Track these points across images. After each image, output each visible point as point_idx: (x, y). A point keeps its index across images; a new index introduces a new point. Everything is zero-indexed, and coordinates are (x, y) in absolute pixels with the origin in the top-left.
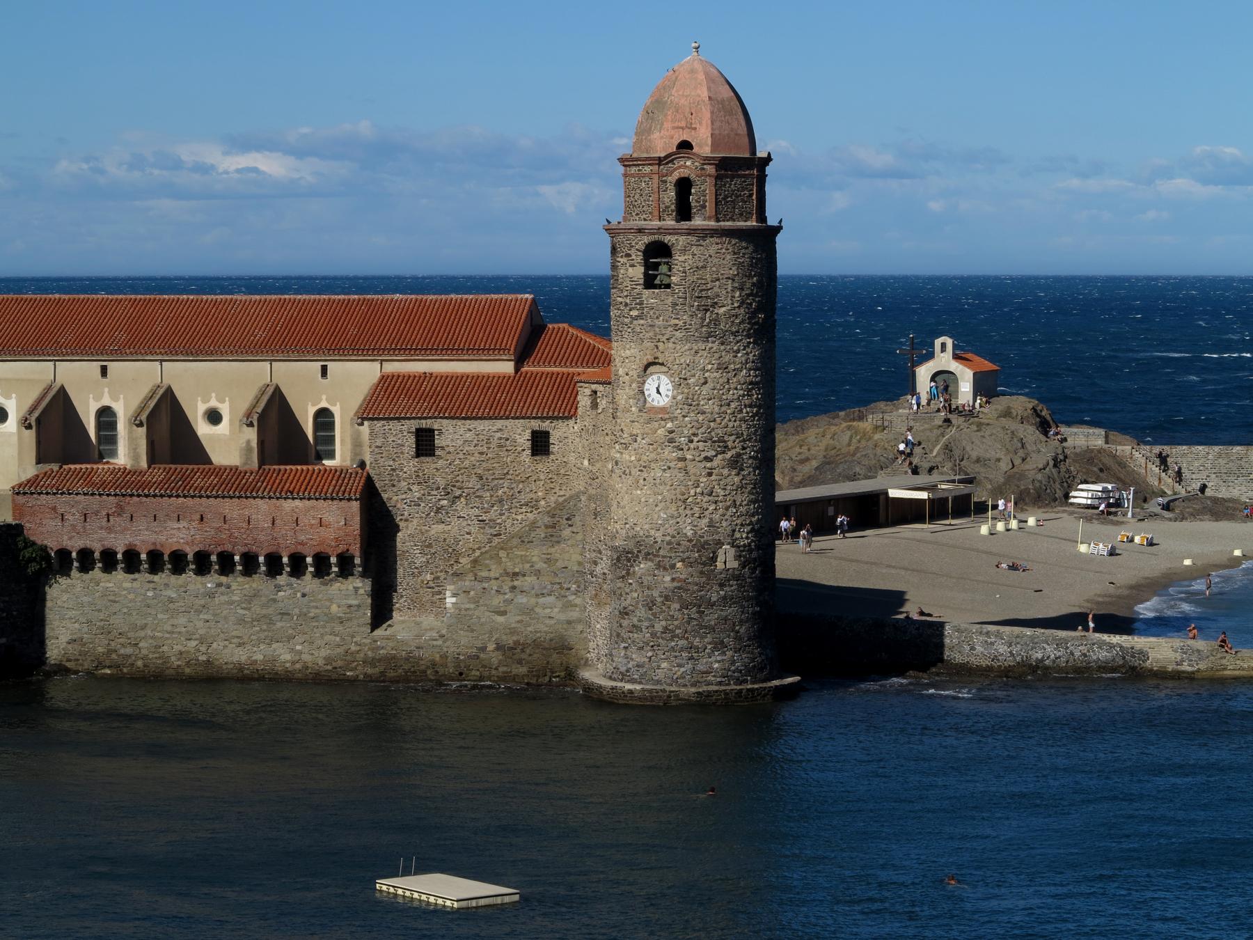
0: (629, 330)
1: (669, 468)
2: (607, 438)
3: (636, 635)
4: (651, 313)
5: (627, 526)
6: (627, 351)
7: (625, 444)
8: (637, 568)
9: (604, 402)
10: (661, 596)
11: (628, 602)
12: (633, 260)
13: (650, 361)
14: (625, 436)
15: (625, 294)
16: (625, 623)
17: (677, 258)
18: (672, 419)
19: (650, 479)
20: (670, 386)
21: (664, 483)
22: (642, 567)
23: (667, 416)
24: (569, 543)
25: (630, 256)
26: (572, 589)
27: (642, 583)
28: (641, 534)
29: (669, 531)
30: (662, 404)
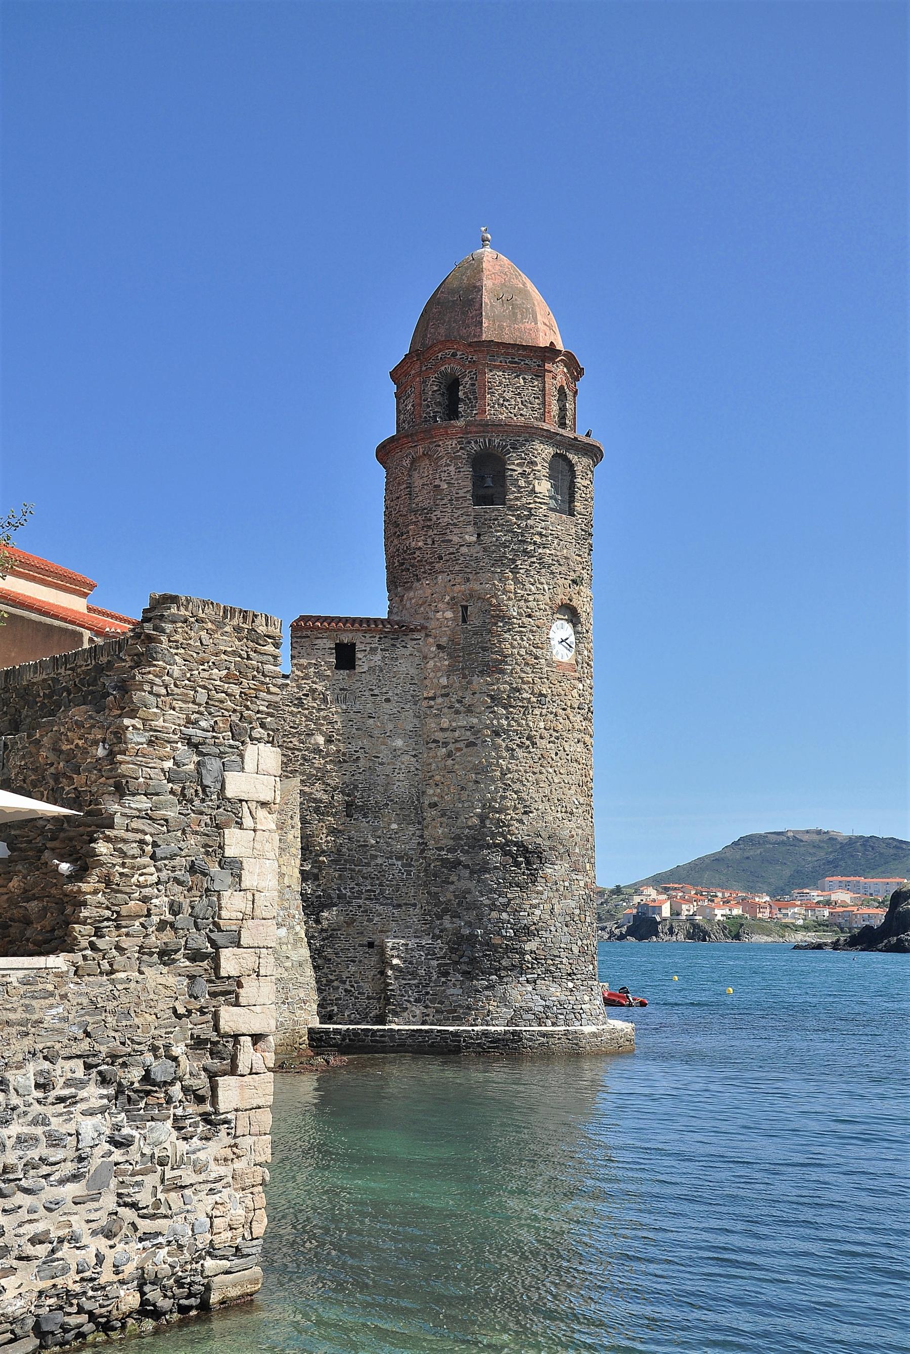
0: (534, 559)
2: (385, 705)
4: (556, 541)
5: (530, 814)
6: (528, 586)
7: (523, 707)
8: (549, 871)
11: (536, 919)
13: (565, 602)
14: (525, 695)
15: (526, 513)
16: (527, 947)
17: (579, 480)
19: (561, 753)
20: (572, 639)
22: (556, 870)
23: (577, 675)
24: (293, 850)
26: (297, 916)
27: (557, 890)
30: (565, 660)
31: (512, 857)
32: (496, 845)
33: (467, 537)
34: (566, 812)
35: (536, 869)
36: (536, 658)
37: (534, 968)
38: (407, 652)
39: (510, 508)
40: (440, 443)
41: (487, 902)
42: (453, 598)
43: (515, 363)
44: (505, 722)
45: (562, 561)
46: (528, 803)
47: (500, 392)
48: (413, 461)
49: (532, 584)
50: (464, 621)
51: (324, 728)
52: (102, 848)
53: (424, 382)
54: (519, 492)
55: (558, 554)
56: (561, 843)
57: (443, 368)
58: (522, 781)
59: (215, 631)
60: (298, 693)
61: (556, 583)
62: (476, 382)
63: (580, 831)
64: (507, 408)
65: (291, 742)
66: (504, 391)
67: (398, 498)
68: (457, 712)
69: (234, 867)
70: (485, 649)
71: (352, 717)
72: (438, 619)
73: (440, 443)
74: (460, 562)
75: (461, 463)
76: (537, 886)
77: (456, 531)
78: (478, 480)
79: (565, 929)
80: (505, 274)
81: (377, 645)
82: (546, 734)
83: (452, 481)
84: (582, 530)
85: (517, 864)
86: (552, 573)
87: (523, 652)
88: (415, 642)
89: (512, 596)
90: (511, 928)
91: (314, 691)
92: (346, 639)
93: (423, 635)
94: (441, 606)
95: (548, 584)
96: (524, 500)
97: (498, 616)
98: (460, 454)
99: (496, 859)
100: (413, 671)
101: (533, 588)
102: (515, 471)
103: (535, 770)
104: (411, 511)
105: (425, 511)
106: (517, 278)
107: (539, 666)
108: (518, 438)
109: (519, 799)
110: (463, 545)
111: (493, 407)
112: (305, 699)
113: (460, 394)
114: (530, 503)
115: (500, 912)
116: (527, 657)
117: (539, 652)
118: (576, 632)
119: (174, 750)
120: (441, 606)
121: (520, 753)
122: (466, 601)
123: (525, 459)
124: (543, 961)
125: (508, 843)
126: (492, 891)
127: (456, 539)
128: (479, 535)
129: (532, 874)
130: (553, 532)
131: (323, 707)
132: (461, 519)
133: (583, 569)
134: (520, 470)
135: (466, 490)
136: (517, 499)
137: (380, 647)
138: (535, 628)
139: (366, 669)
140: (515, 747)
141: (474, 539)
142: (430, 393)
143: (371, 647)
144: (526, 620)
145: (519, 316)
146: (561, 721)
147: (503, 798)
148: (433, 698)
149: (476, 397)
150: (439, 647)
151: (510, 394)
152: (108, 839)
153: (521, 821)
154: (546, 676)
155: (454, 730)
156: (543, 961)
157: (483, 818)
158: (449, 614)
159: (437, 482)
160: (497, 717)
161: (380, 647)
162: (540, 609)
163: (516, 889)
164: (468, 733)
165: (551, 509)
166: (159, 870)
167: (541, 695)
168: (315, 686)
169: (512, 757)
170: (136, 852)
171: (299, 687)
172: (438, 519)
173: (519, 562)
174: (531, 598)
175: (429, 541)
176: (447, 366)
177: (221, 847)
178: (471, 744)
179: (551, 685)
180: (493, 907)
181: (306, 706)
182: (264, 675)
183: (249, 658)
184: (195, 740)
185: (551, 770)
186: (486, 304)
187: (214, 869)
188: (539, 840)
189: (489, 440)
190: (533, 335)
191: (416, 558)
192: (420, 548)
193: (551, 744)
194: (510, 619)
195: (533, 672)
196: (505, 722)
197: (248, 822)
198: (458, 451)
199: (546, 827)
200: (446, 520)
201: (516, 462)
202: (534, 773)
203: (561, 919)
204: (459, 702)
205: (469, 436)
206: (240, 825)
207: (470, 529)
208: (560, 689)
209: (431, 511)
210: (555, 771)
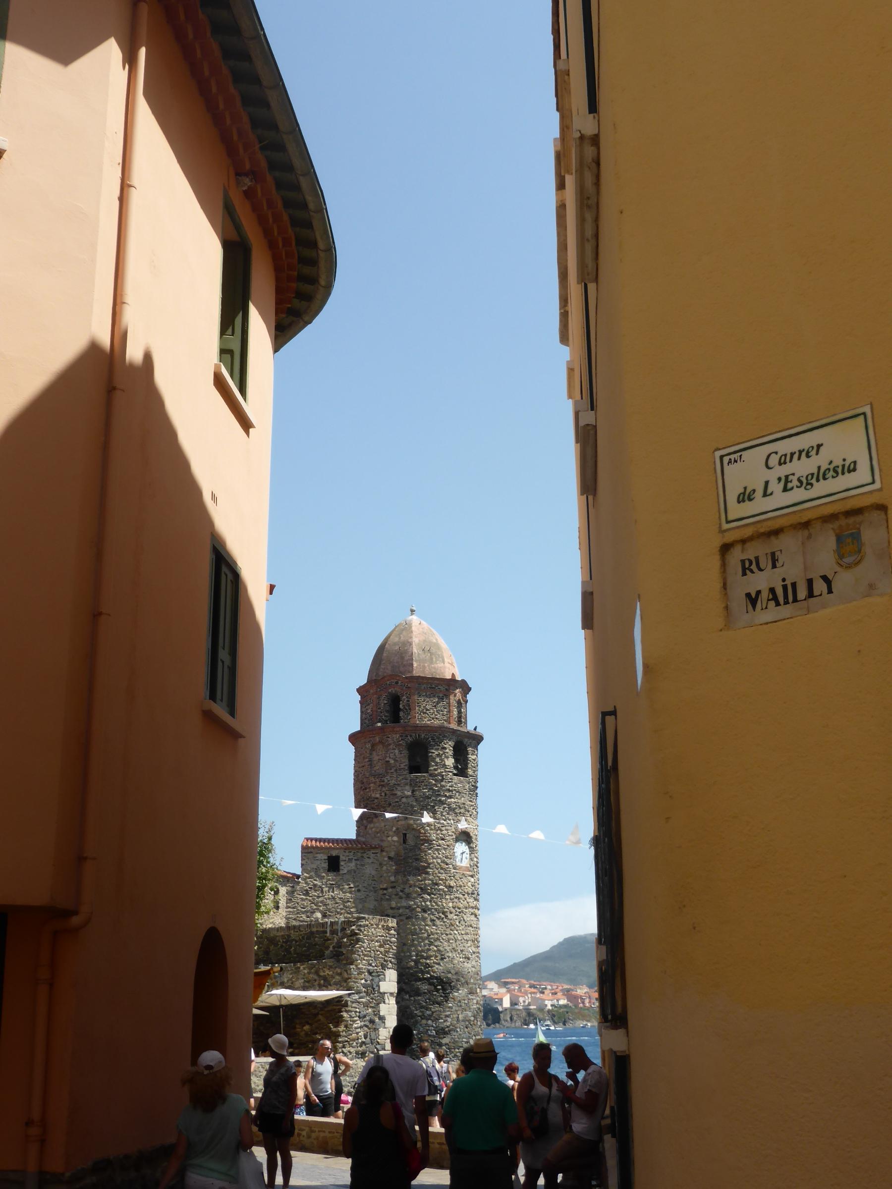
1: (472, 914)
3: (457, 1050)
5: (445, 960)
7: (440, 894)
8: (456, 994)
9: (352, 865)
10: (472, 1016)
11: (448, 1024)
12: (447, 753)
14: (441, 887)
18: (472, 876)
19: (462, 922)
20: (468, 851)
21: (471, 926)
22: (461, 993)
23: (471, 873)
25: (445, 748)
27: (461, 1006)
28: (459, 966)
29: (474, 963)
31: (434, 986)
32: (425, 979)
33: (406, 792)
34: (465, 958)
35: (448, 994)
36: (447, 864)
37: (448, 1055)
38: (370, 861)
39: (431, 775)
40: (390, 736)
41: (420, 1014)
42: (397, 829)
43: (433, 688)
44: (428, 903)
45: (462, 806)
46: (443, 953)
47: (424, 705)
48: (373, 746)
49: (445, 820)
50: (405, 841)
51: (321, 908)
52: (345, 1014)
53: (379, 698)
54: (436, 766)
55: (459, 801)
56: (463, 977)
57: (390, 690)
58: (439, 940)
59: (376, 928)
60: (306, 887)
61: (458, 819)
62: (410, 700)
63: (473, 969)
64: (428, 715)
65: (301, 917)
66: (426, 705)
67: (363, 766)
68: (401, 898)
69: (382, 1019)
70: (417, 859)
71: (338, 901)
72: (389, 841)
73: (390, 736)
74: (401, 807)
75: (402, 748)
76: (449, 1004)
77: (399, 788)
78: (411, 758)
79: (466, 1030)
80: (426, 634)
81: (352, 857)
82: (453, 911)
83: (397, 759)
84: (472, 786)
85: (437, 990)
86: (456, 813)
87: (439, 861)
88: (375, 855)
89: (433, 827)
90: (434, 1030)
91: (315, 885)
92: (334, 853)
93: (380, 851)
94: (391, 833)
95: (454, 820)
96: (439, 771)
97: (425, 840)
98: (401, 743)
99: (425, 987)
100: (374, 873)
101: (445, 822)
102: (434, 753)
103: (447, 932)
104: (371, 775)
105: (381, 776)
106: (432, 636)
107: (449, 869)
108: (435, 734)
109: (439, 950)
110: (403, 797)
111: (420, 714)
112: (310, 891)
113: (401, 706)
114: (443, 772)
115: (428, 1020)
116: (442, 864)
117: (448, 861)
118: (470, 848)
119: (365, 975)
120: (391, 833)
121: (438, 922)
122: (406, 831)
123: (439, 746)
124: (453, 1050)
125: (432, 977)
126: (422, 1007)
127: (399, 793)
128: (413, 791)
129: (446, 997)
130: (456, 788)
131: (321, 895)
132: (402, 782)
133: (473, 809)
134: (437, 753)
135: (405, 764)
136: (435, 770)
137: (354, 858)
138: (446, 847)
139: (346, 872)
140: (435, 919)
141: (410, 793)
142: (383, 704)
143: (349, 859)
144: (440, 842)
145: (434, 660)
146: (462, 902)
147: (429, 950)
148: (386, 889)
149: (409, 709)
150: (390, 858)
151: (430, 706)
152: (347, 1011)
153: (439, 964)
154: (453, 875)
155: (399, 909)
156: (453, 1050)
157: (417, 962)
158: (395, 838)
159: (387, 760)
160: (425, 901)
161: (354, 858)
162: (449, 835)
163: (437, 1005)
164: (407, 911)
165: (455, 775)
166: (361, 1022)
167: (450, 887)
168: (315, 882)
169: (434, 925)
170: (354, 1015)
171: (306, 883)
172: (389, 781)
173: (436, 808)
174: (443, 828)
175: (383, 794)
176: (392, 689)
177: (379, 1011)
178: (408, 918)
179: (456, 881)
180: (423, 1017)
181: (311, 895)
182: (391, 943)
183: (387, 937)
184: (371, 971)
185: (456, 932)
186: (415, 653)
187: (377, 1020)
188: (449, 975)
189: (418, 735)
190: (442, 671)
191: (374, 804)
192: (377, 798)
193: (456, 916)
194: (431, 841)
195: (446, 873)
196: (428, 903)
197: (387, 1001)
198: (400, 741)
199: (454, 967)
200: (393, 781)
201: (434, 748)
202: (447, 935)
203: (463, 1023)
204: (402, 891)
205: (407, 732)
206: (384, 1002)
207: (407, 787)
208: (461, 883)
209: (384, 776)
210: (459, 933)
